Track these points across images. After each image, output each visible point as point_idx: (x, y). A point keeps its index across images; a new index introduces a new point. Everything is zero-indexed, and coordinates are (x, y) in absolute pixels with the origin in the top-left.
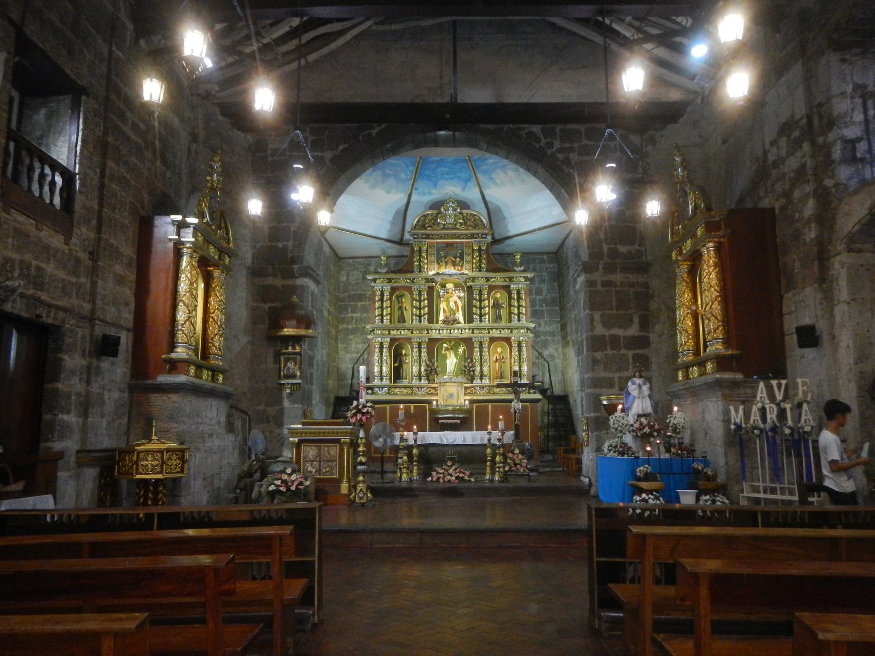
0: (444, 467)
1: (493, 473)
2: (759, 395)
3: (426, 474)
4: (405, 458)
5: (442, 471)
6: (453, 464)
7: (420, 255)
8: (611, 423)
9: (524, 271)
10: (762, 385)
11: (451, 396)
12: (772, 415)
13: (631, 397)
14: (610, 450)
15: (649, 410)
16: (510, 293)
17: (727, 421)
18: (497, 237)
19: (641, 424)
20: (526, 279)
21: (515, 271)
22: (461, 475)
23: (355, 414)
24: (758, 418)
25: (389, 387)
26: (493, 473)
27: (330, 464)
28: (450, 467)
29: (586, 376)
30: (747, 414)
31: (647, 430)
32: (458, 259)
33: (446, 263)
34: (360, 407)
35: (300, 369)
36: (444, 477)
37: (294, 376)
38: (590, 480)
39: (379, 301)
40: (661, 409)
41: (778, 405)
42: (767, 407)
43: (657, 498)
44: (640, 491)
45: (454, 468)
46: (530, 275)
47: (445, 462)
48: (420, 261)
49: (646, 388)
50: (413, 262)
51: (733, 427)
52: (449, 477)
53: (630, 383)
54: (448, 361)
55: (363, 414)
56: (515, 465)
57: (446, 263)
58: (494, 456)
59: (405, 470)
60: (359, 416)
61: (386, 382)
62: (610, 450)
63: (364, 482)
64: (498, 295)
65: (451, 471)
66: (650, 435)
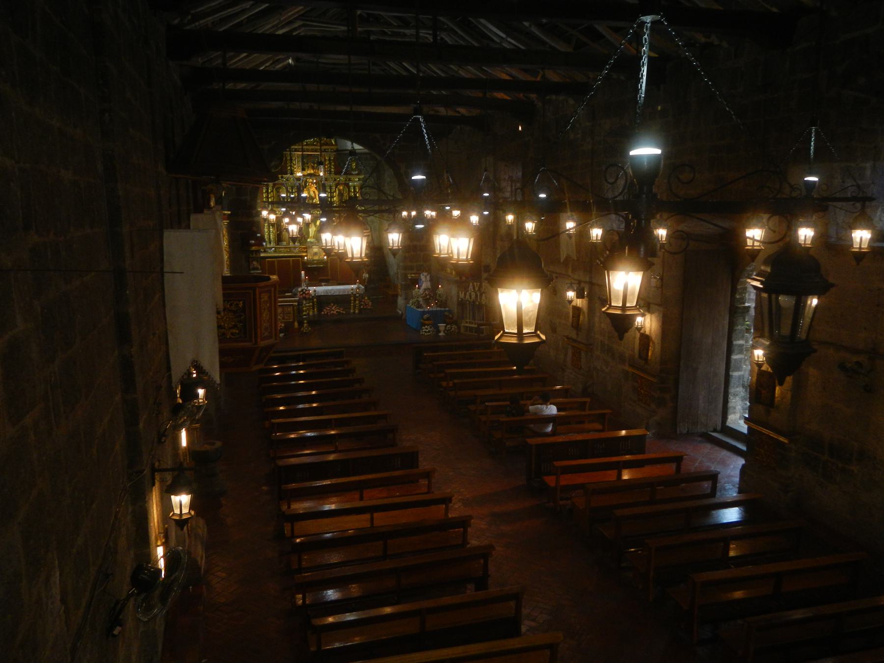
0: (330, 306)
1: (354, 309)
2: (470, 288)
3: (320, 310)
4: (311, 304)
5: (329, 309)
6: (334, 305)
7: (291, 162)
8: (414, 293)
9: (358, 174)
10: (471, 284)
11: (316, 254)
12: (473, 297)
13: (422, 281)
14: (412, 304)
15: (430, 287)
16: (349, 187)
17: (458, 296)
18: (340, 149)
19: (426, 294)
20: (359, 179)
21: (352, 174)
22: (339, 310)
23: (302, 294)
24: (469, 297)
25: (275, 248)
26: (354, 309)
27: (288, 315)
28: (333, 306)
29: (401, 264)
30: (465, 294)
31: (428, 297)
32: (316, 165)
33: (308, 167)
34: (304, 291)
35: (261, 265)
36: (330, 312)
37: (257, 269)
38: (402, 312)
39: (265, 192)
40: (434, 287)
41: (476, 293)
42: (472, 293)
43: (430, 328)
44: (424, 325)
45: (334, 307)
46: (362, 177)
47: (330, 304)
48: (291, 166)
49: (428, 277)
50: (287, 167)
51: (460, 300)
52: (332, 312)
53: (421, 275)
54: (310, 230)
55: (306, 294)
56: (366, 305)
57: (308, 167)
58: (355, 301)
59: (311, 310)
60: (304, 295)
61: (272, 245)
62: (412, 304)
63: (306, 323)
64: (341, 188)
65: (333, 309)
66: (429, 299)
